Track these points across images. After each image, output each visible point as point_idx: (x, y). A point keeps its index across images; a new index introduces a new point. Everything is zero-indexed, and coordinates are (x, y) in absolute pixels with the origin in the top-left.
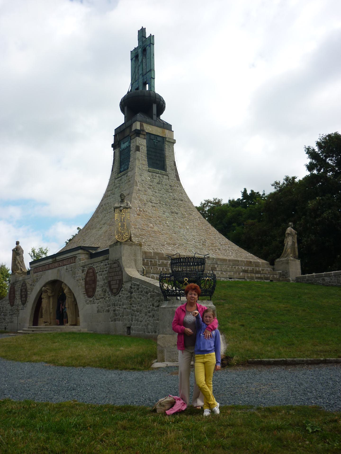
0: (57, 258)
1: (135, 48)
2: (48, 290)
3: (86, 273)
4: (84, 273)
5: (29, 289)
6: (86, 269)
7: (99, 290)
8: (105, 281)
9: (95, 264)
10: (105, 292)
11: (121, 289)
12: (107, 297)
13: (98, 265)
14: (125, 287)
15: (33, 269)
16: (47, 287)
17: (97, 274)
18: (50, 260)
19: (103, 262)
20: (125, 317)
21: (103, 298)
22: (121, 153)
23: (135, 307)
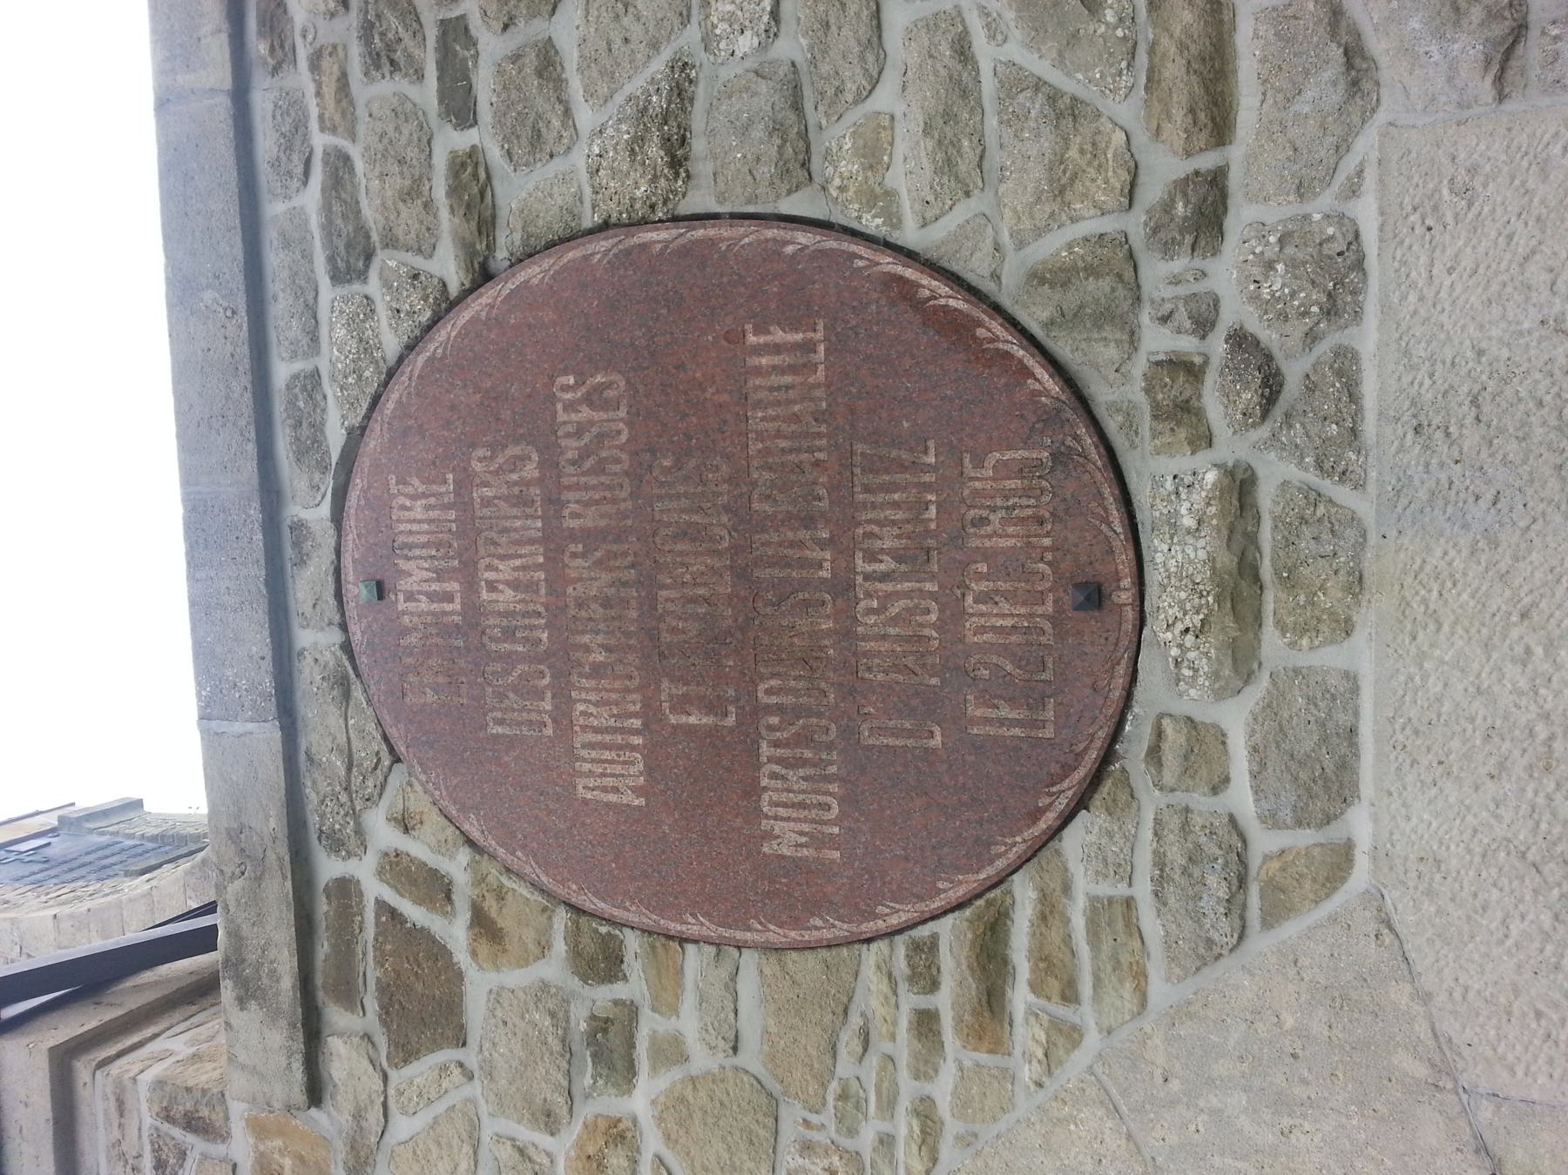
3: (457, 866)
4: (455, 933)
9: (282, 371)
13: (311, 198)
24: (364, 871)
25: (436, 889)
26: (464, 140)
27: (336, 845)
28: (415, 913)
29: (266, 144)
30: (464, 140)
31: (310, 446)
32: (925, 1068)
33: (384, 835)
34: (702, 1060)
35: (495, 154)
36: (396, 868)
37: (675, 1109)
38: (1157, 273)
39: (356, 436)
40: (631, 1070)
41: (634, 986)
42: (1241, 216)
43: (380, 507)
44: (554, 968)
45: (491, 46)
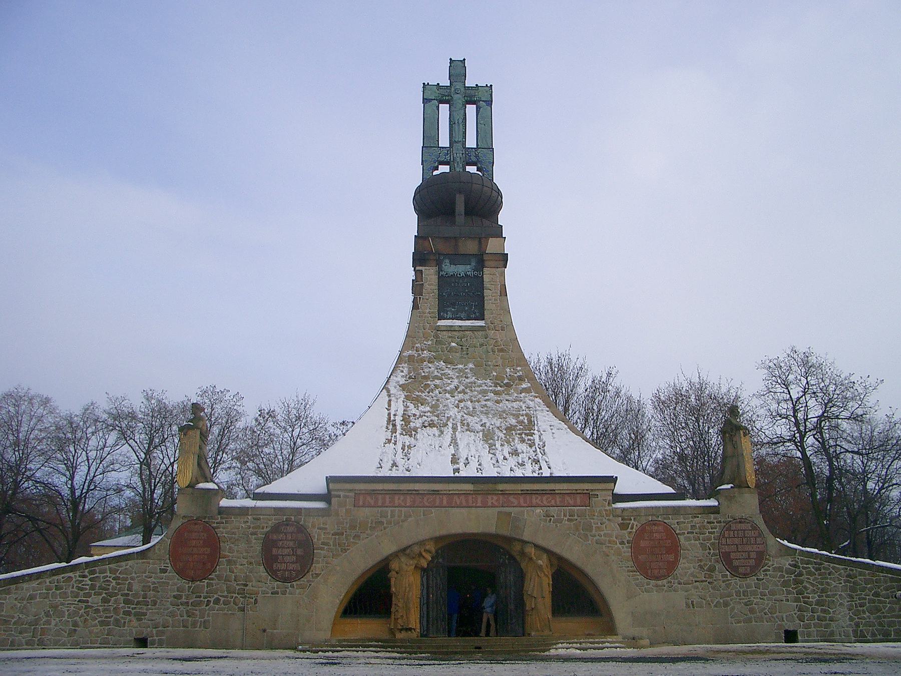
0: (501, 487)
1: (438, 84)
2: (424, 554)
4: (629, 530)
5: (323, 543)
6: (635, 524)
7: (686, 567)
8: (712, 551)
10: (712, 569)
11: (763, 567)
12: (720, 580)
13: (682, 520)
14: (773, 565)
15: (352, 494)
16: (427, 547)
17: (682, 538)
18: (469, 487)
19: (700, 516)
20: (778, 614)
21: (704, 581)
22: (443, 281)
23: (813, 598)
24: (633, 521)
25: (632, 528)
26: (686, 533)
27: (634, 519)
28: (630, 526)
29: (686, 516)
30: (686, 533)
31: (665, 519)
32: (625, 567)
33: (635, 523)
34: (623, 550)
35: (685, 536)
36: (633, 524)
37: (619, 548)
38: (676, 581)
39: (665, 523)
40: (621, 544)
41: (627, 545)
42: (679, 585)
43: (660, 524)
44: (628, 538)
45: (691, 535)
